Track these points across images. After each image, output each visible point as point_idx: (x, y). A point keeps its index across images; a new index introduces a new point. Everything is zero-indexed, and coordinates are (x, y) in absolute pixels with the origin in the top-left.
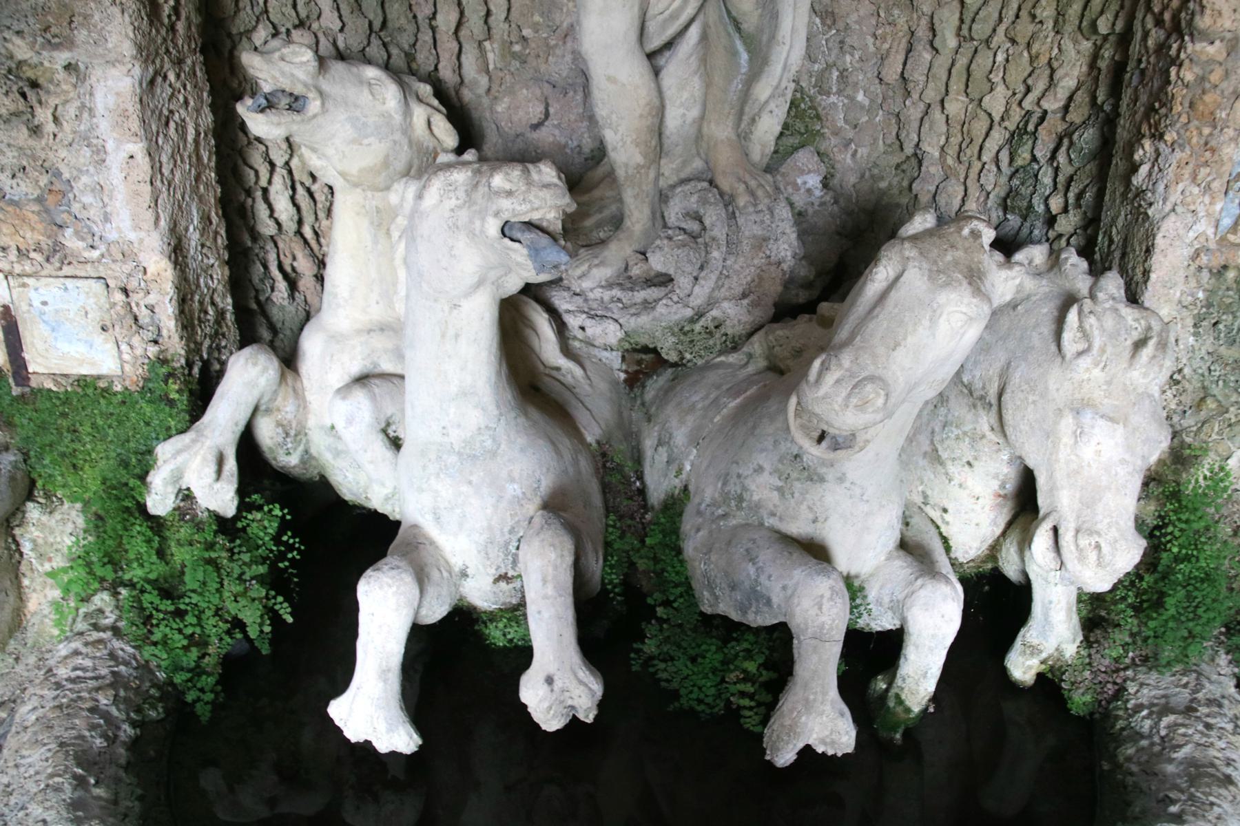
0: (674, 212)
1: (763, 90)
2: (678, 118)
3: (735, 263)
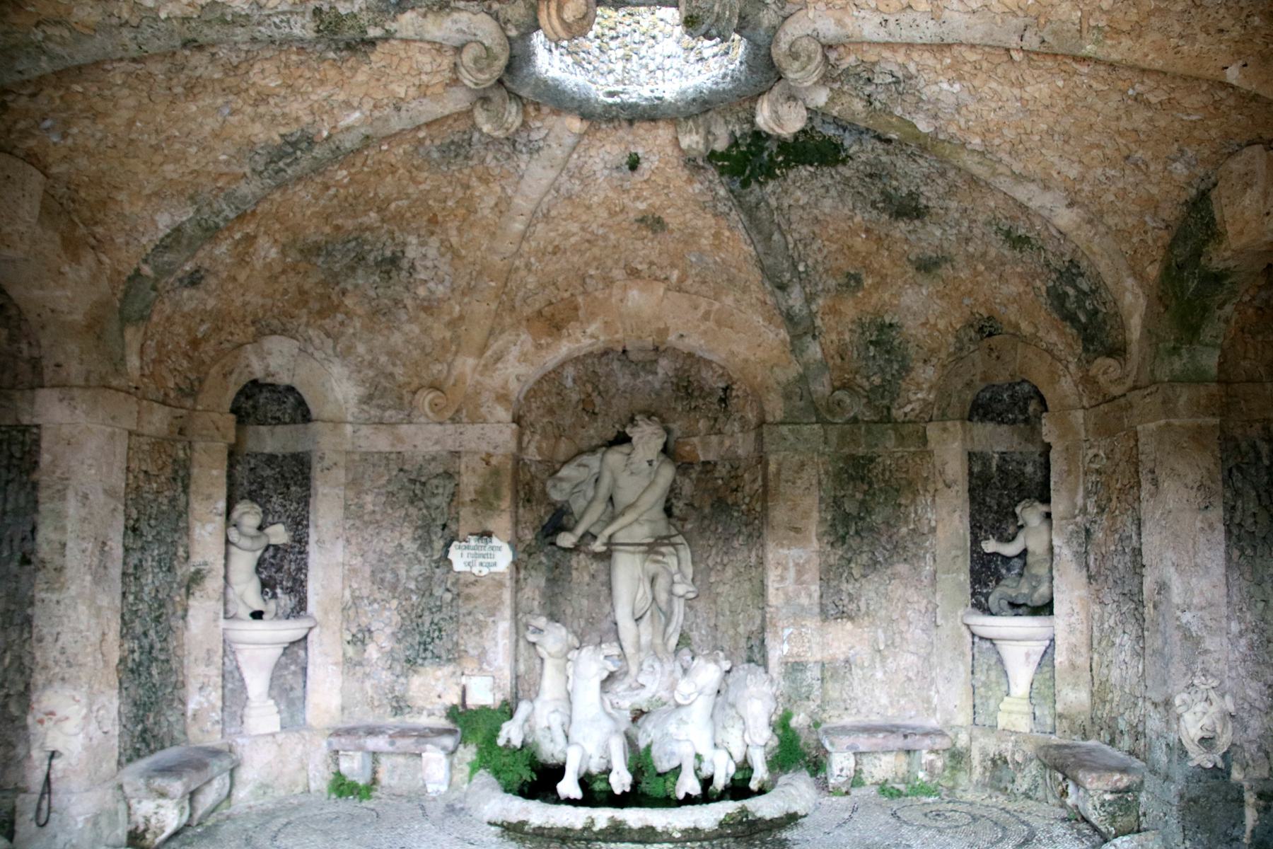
0: (645, 666)
1: (670, 629)
2: (645, 639)
3: (664, 679)
